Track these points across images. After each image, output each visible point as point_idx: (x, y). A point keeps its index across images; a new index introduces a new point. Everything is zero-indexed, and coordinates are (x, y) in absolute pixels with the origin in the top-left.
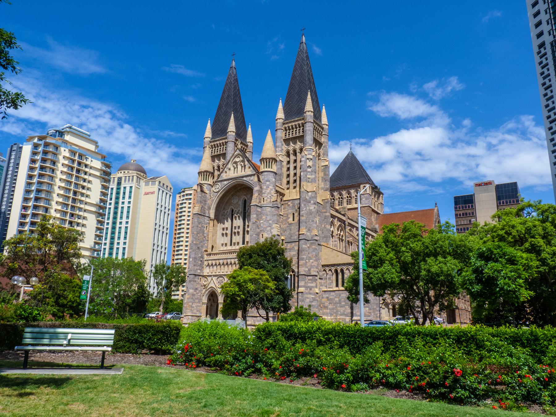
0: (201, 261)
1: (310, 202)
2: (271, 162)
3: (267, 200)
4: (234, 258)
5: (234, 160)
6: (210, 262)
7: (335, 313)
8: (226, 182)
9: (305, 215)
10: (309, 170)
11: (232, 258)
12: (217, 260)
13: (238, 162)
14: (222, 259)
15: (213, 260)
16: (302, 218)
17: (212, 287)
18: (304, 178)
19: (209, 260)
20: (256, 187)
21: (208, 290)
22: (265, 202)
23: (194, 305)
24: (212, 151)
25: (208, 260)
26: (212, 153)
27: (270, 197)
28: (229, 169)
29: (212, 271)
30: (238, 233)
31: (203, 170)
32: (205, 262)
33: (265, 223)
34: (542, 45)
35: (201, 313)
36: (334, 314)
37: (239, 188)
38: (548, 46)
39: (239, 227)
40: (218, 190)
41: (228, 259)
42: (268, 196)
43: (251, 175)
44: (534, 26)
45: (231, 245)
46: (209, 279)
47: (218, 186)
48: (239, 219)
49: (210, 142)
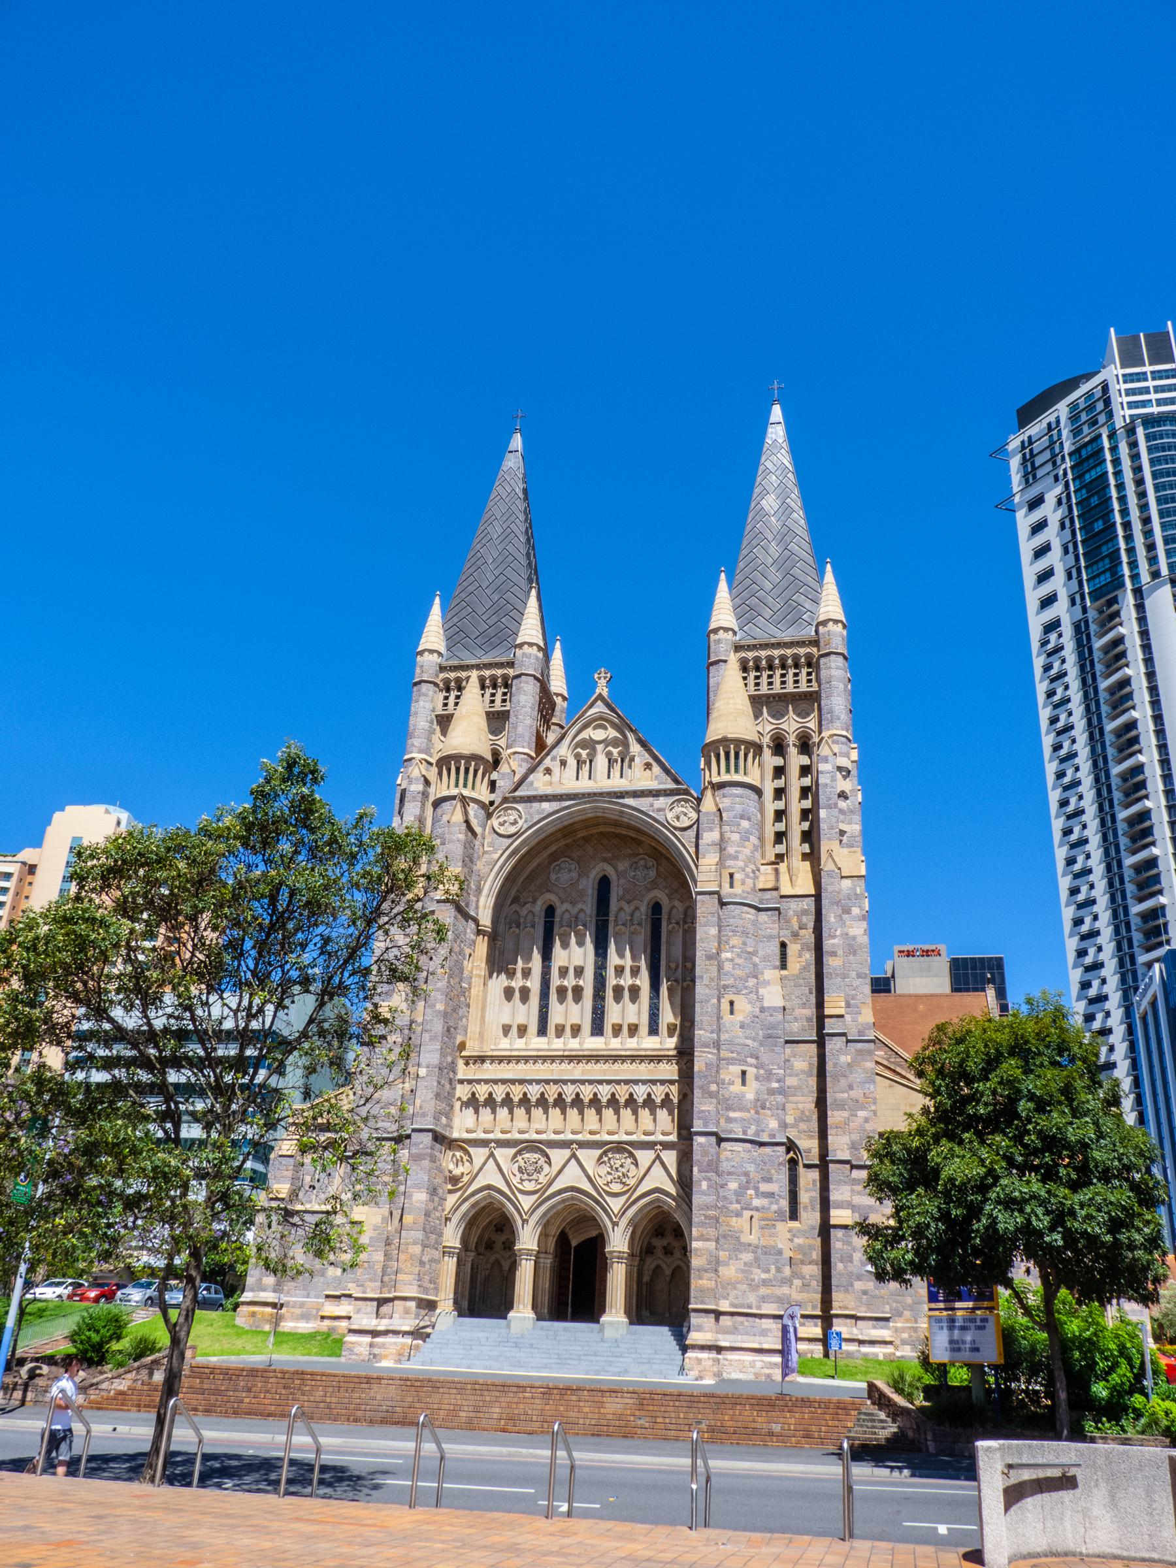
0: (451, 1080)
1: (847, 911)
2: (742, 754)
3: (743, 883)
4: (663, 1082)
5: (584, 735)
6: (482, 1091)
7: (911, 1308)
8: (547, 807)
9: (840, 952)
10: (842, 804)
11: (583, 1082)
12: (513, 1082)
13: (599, 742)
14: (538, 1082)
15: (496, 1082)
16: (830, 963)
17: (489, 1187)
18: (831, 828)
19: (479, 1081)
20: (711, 830)
21: (472, 1200)
22: (738, 889)
23: (425, 1259)
24: (446, 698)
25: (470, 1082)
26: (446, 705)
27: (753, 872)
28: (563, 763)
29: (488, 1126)
30: (578, 992)
31: (466, 752)
32: (459, 1087)
33: (740, 961)
34: (1052, 626)
35: (437, 1290)
36: (907, 1314)
37: (581, 834)
38: (1067, 629)
39: (579, 972)
40: (513, 830)
41: (565, 1082)
42: (748, 870)
43: (656, 794)
44: (1035, 577)
45: (542, 1031)
46: (479, 1154)
47: (513, 815)
48: (581, 943)
49: (442, 669)
